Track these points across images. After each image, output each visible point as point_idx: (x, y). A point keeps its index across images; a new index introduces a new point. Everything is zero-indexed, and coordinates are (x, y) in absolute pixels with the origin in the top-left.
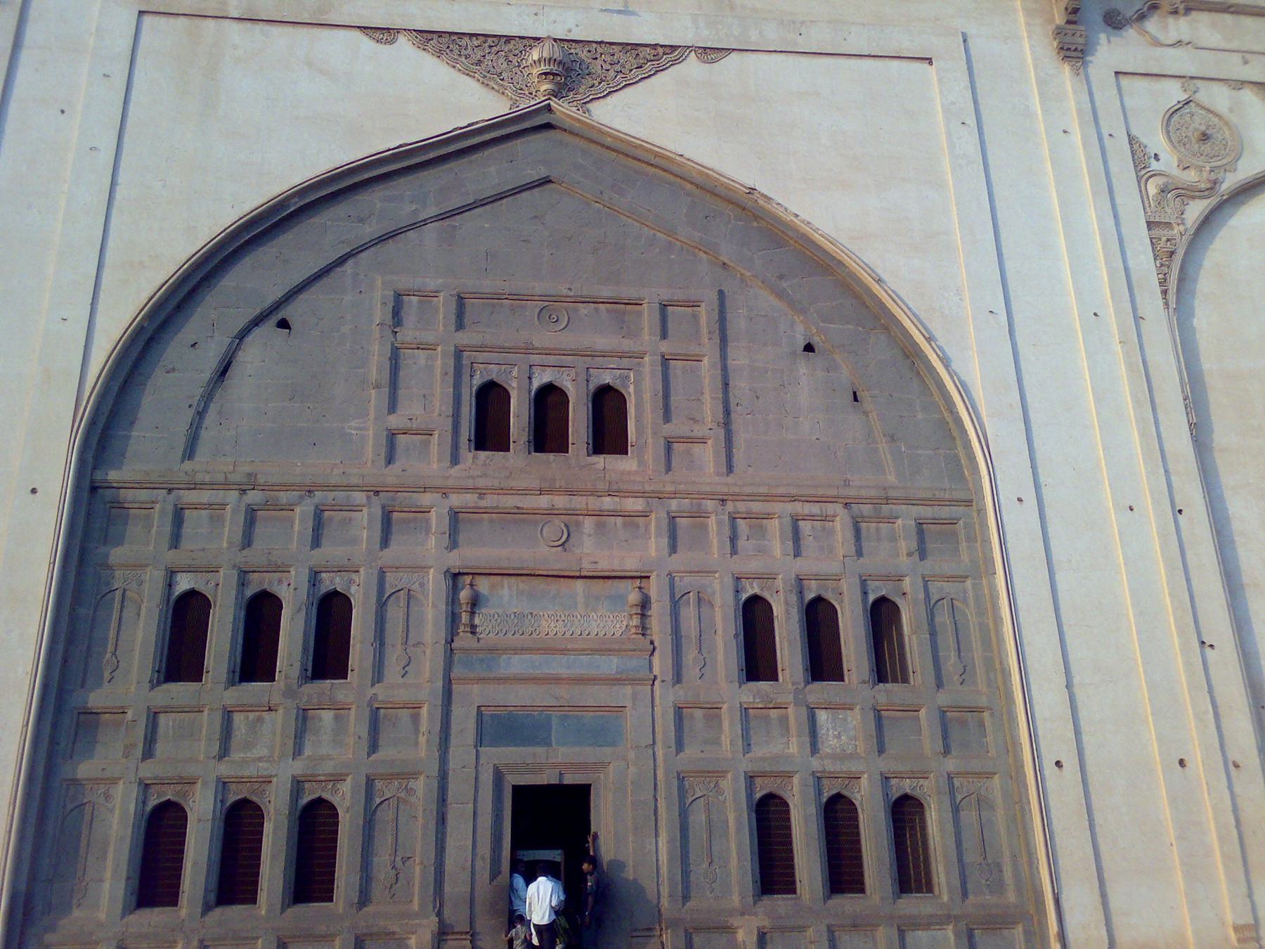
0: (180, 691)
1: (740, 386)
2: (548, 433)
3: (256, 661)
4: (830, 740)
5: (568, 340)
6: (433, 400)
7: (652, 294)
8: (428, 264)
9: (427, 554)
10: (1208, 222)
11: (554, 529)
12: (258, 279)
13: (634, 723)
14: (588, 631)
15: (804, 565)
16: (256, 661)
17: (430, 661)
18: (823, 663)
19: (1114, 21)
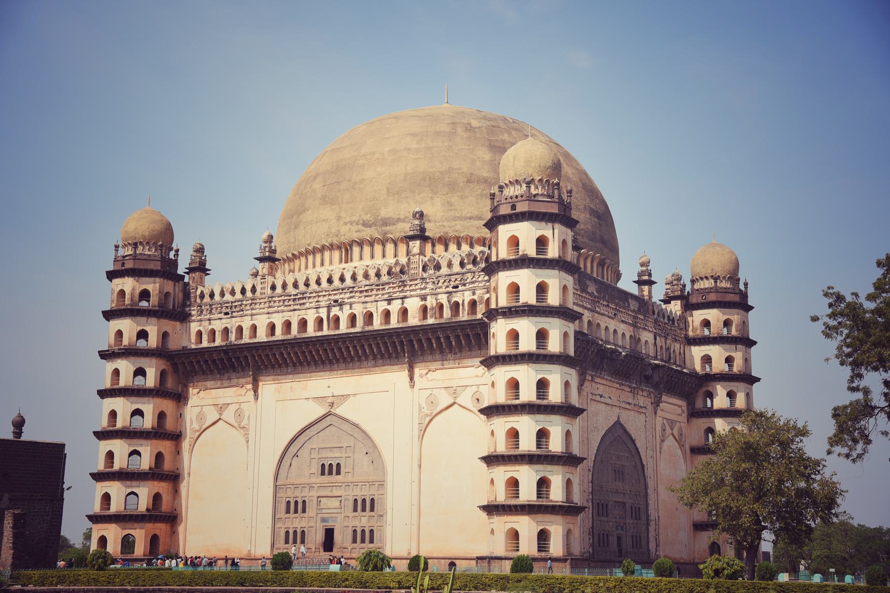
0: (288, 515)
1: (356, 461)
2: (330, 473)
3: (296, 512)
4: (363, 521)
5: (333, 455)
6: (316, 469)
7: (345, 445)
8: (315, 443)
9: (314, 494)
10: (431, 420)
12: (293, 449)
13: (339, 520)
14: (332, 507)
15: (362, 493)
16: (296, 512)
17: (315, 510)
18: (364, 510)
19: (421, 376)
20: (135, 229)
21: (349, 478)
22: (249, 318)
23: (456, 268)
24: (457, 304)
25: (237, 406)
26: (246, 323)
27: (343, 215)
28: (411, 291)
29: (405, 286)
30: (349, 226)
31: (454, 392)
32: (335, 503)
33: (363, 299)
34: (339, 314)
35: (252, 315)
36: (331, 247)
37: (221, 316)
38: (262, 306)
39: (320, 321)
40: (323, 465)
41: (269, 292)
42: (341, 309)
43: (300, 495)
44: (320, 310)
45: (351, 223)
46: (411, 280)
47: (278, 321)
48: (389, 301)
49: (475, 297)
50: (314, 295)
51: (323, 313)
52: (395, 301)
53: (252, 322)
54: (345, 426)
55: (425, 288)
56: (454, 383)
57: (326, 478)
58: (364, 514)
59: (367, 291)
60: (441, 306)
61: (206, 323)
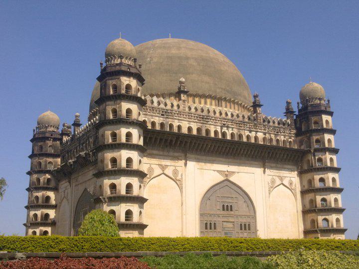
2: (227, 210)
11: (228, 218)
16: (211, 229)
18: (245, 229)
20: (131, 50)
21: (237, 213)
22: (176, 121)
23: (276, 125)
24: (278, 141)
25: (174, 168)
26: (176, 124)
27: (216, 83)
28: (260, 129)
29: (256, 126)
30: (221, 90)
31: (281, 179)
32: (230, 225)
33: (238, 127)
34: (227, 131)
35: (178, 120)
36: (210, 97)
37: (160, 115)
38: (185, 116)
39: (216, 132)
40: (223, 206)
41: (187, 109)
42: (227, 129)
43: (214, 219)
44: (218, 127)
45: (222, 89)
46: (260, 125)
47: (195, 127)
48: (250, 131)
49: (285, 139)
50: (213, 118)
51: (219, 129)
52: (253, 132)
53: (178, 124)
54: (235, 188)
55: (264, 130)
56: (281, 175)
57: (225, 213)
58: (246, 231)
59: (239, 124)
60: (271, 140)
61: (150, 117)
